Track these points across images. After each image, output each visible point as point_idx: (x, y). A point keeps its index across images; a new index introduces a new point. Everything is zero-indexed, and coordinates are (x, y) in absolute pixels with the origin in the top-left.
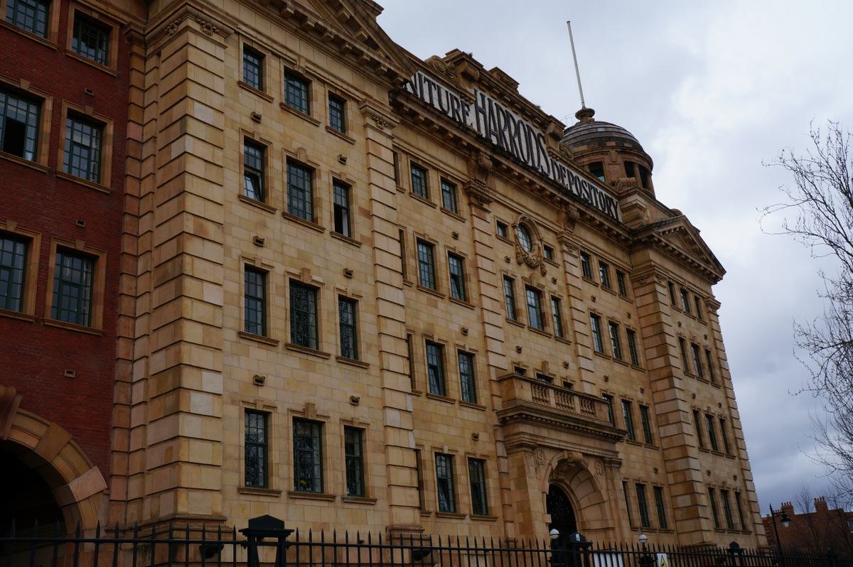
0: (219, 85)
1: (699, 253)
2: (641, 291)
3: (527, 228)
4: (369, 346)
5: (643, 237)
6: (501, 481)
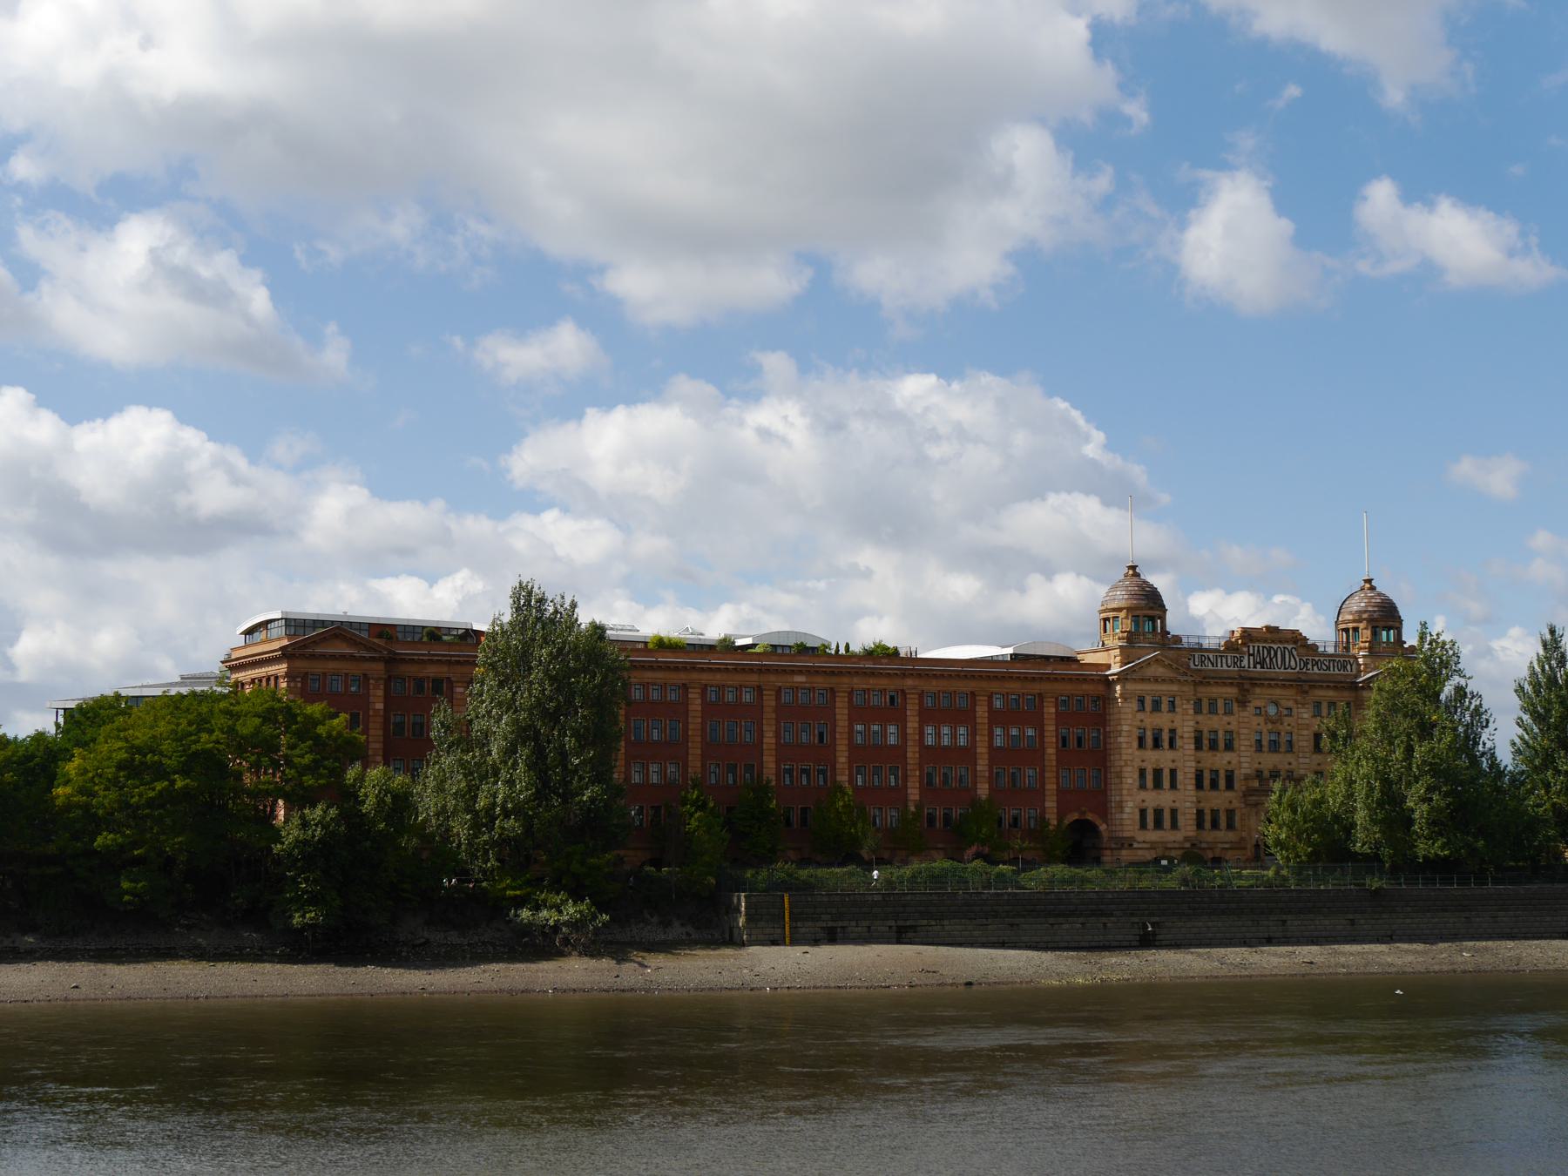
4: (1180, 784)
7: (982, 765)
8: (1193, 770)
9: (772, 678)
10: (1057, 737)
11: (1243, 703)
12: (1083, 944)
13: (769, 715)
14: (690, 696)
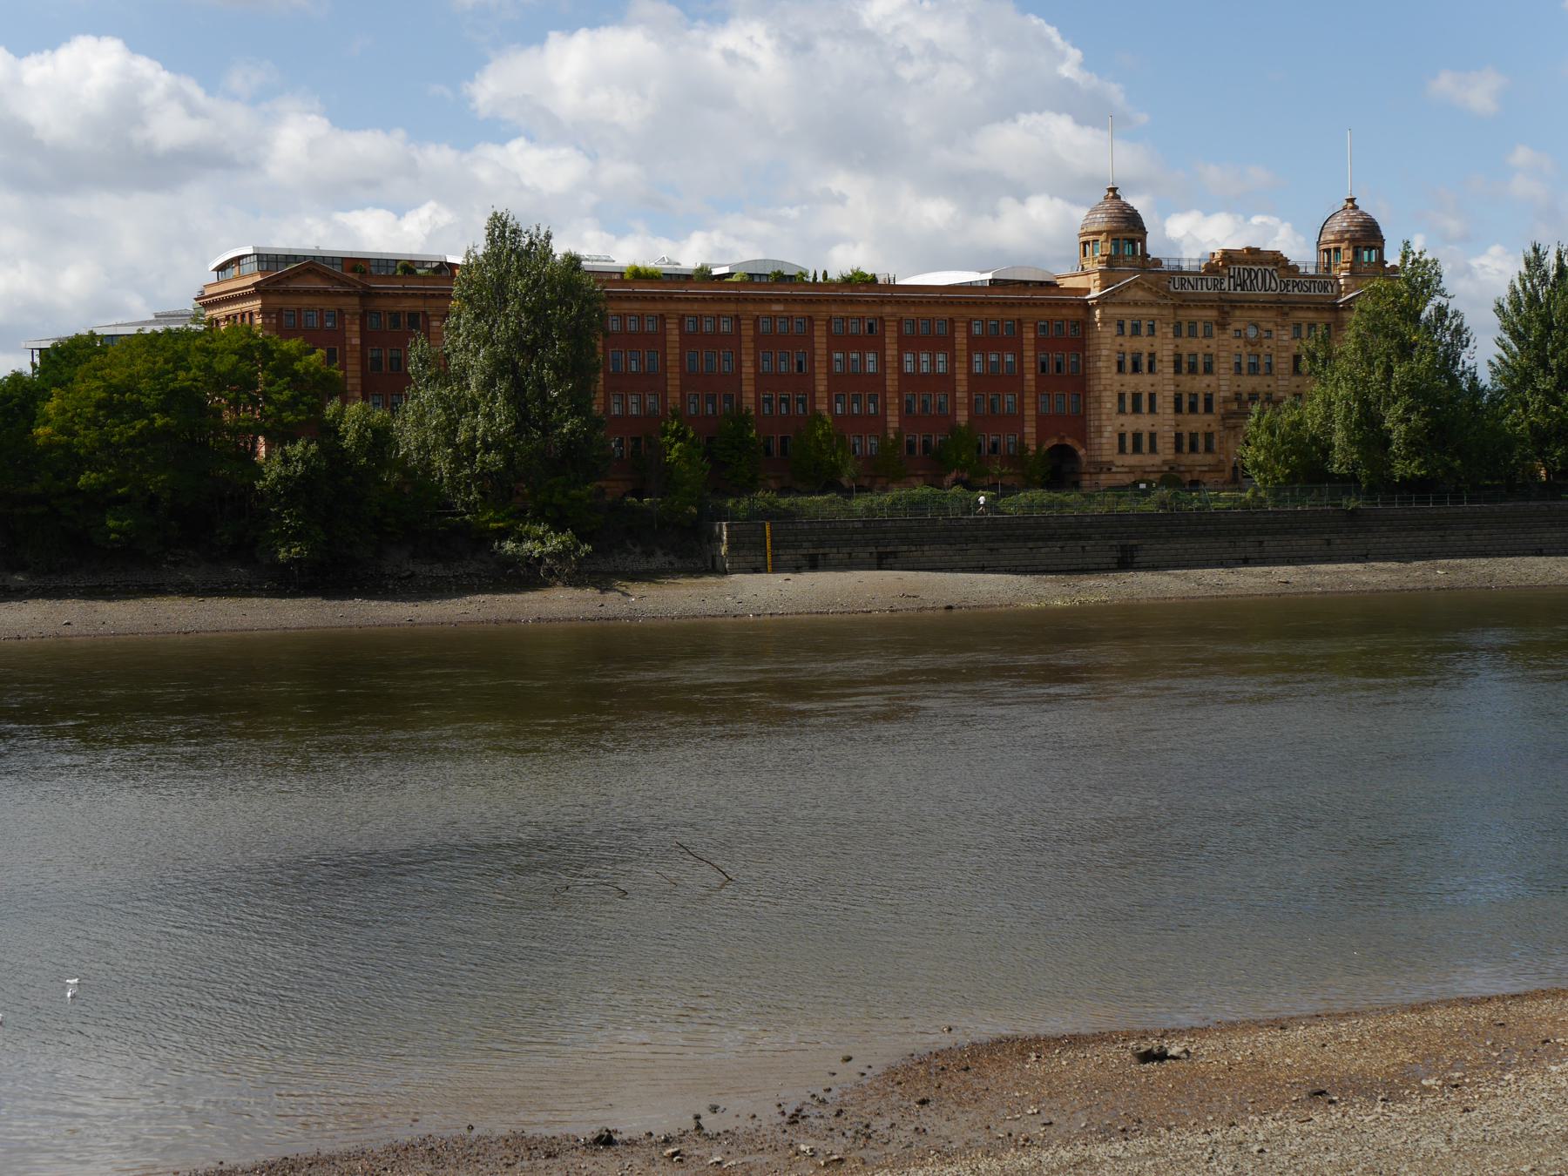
7: (961, 393)
8: (1172, 394)
9: (750, 307)
10: (1036, 362)
11: (1223, 326)
12: (1062, 567)
13: (748, 345)
14: (668, 326)
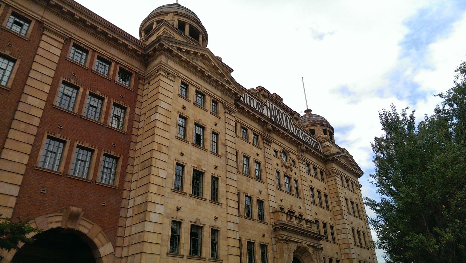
0: (171, 95)
1: (353, 165)
2: (330, 179)
3: (285, 153)
5: (330, 158)
6: (273, 254)
